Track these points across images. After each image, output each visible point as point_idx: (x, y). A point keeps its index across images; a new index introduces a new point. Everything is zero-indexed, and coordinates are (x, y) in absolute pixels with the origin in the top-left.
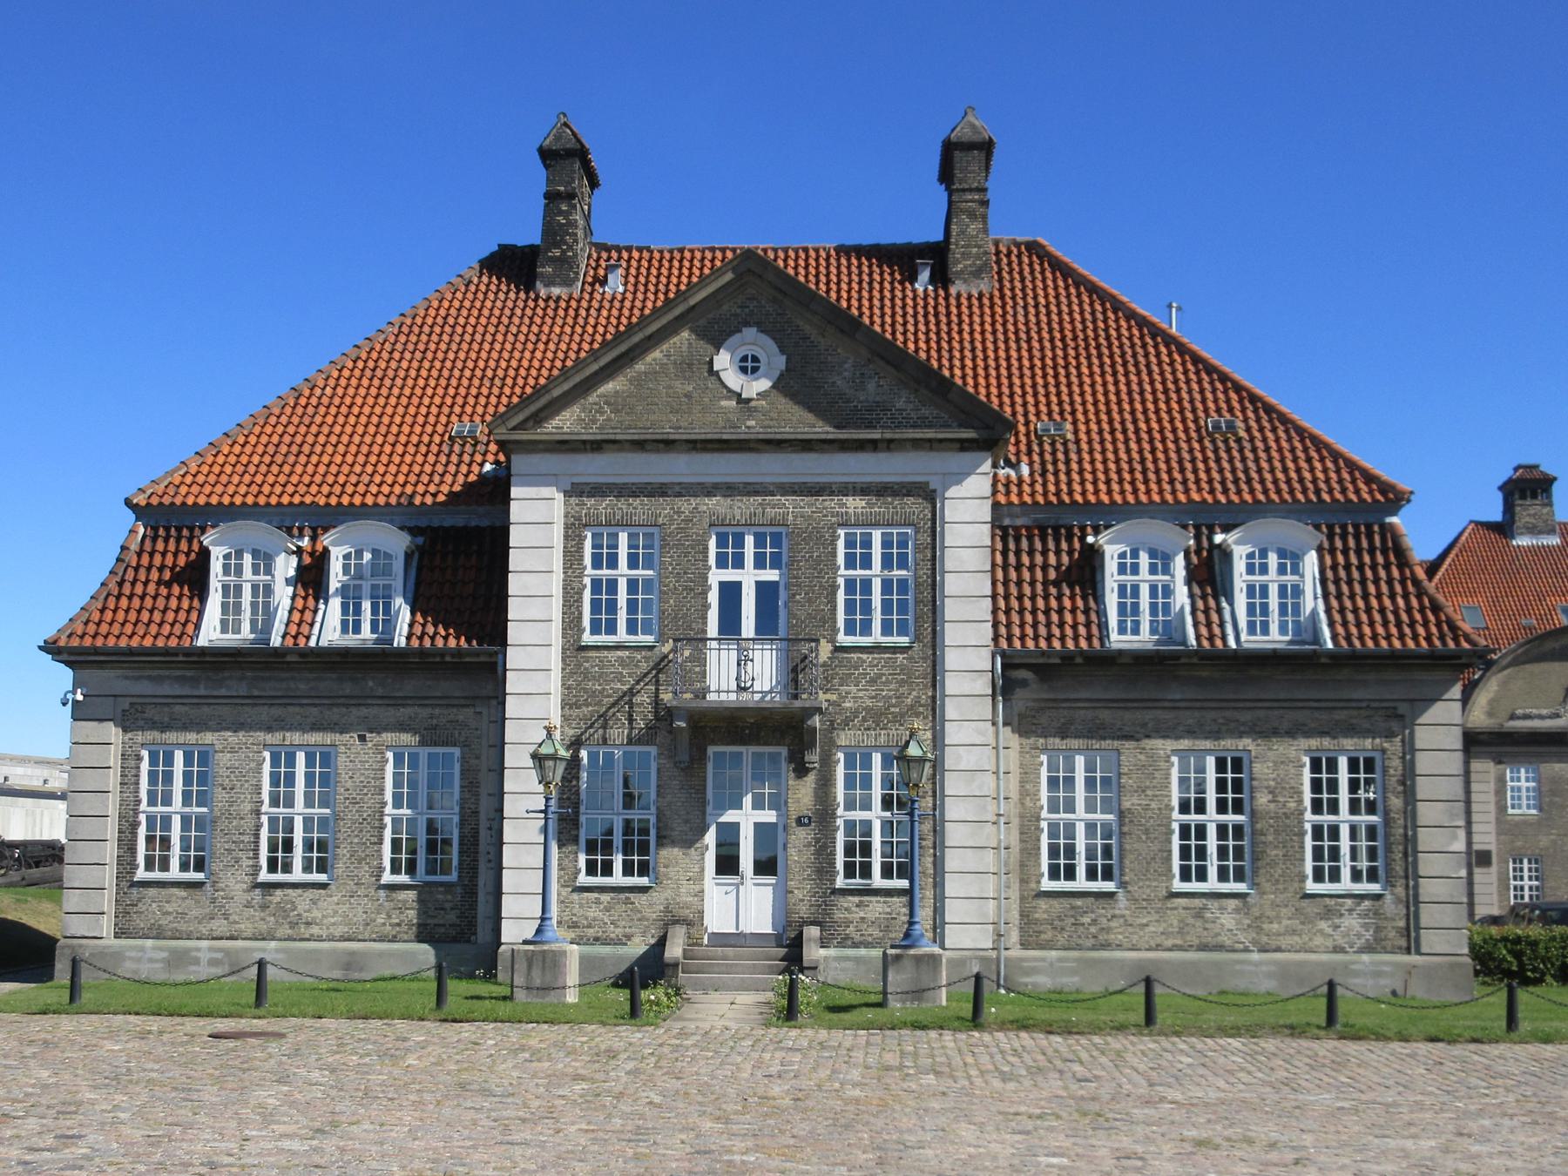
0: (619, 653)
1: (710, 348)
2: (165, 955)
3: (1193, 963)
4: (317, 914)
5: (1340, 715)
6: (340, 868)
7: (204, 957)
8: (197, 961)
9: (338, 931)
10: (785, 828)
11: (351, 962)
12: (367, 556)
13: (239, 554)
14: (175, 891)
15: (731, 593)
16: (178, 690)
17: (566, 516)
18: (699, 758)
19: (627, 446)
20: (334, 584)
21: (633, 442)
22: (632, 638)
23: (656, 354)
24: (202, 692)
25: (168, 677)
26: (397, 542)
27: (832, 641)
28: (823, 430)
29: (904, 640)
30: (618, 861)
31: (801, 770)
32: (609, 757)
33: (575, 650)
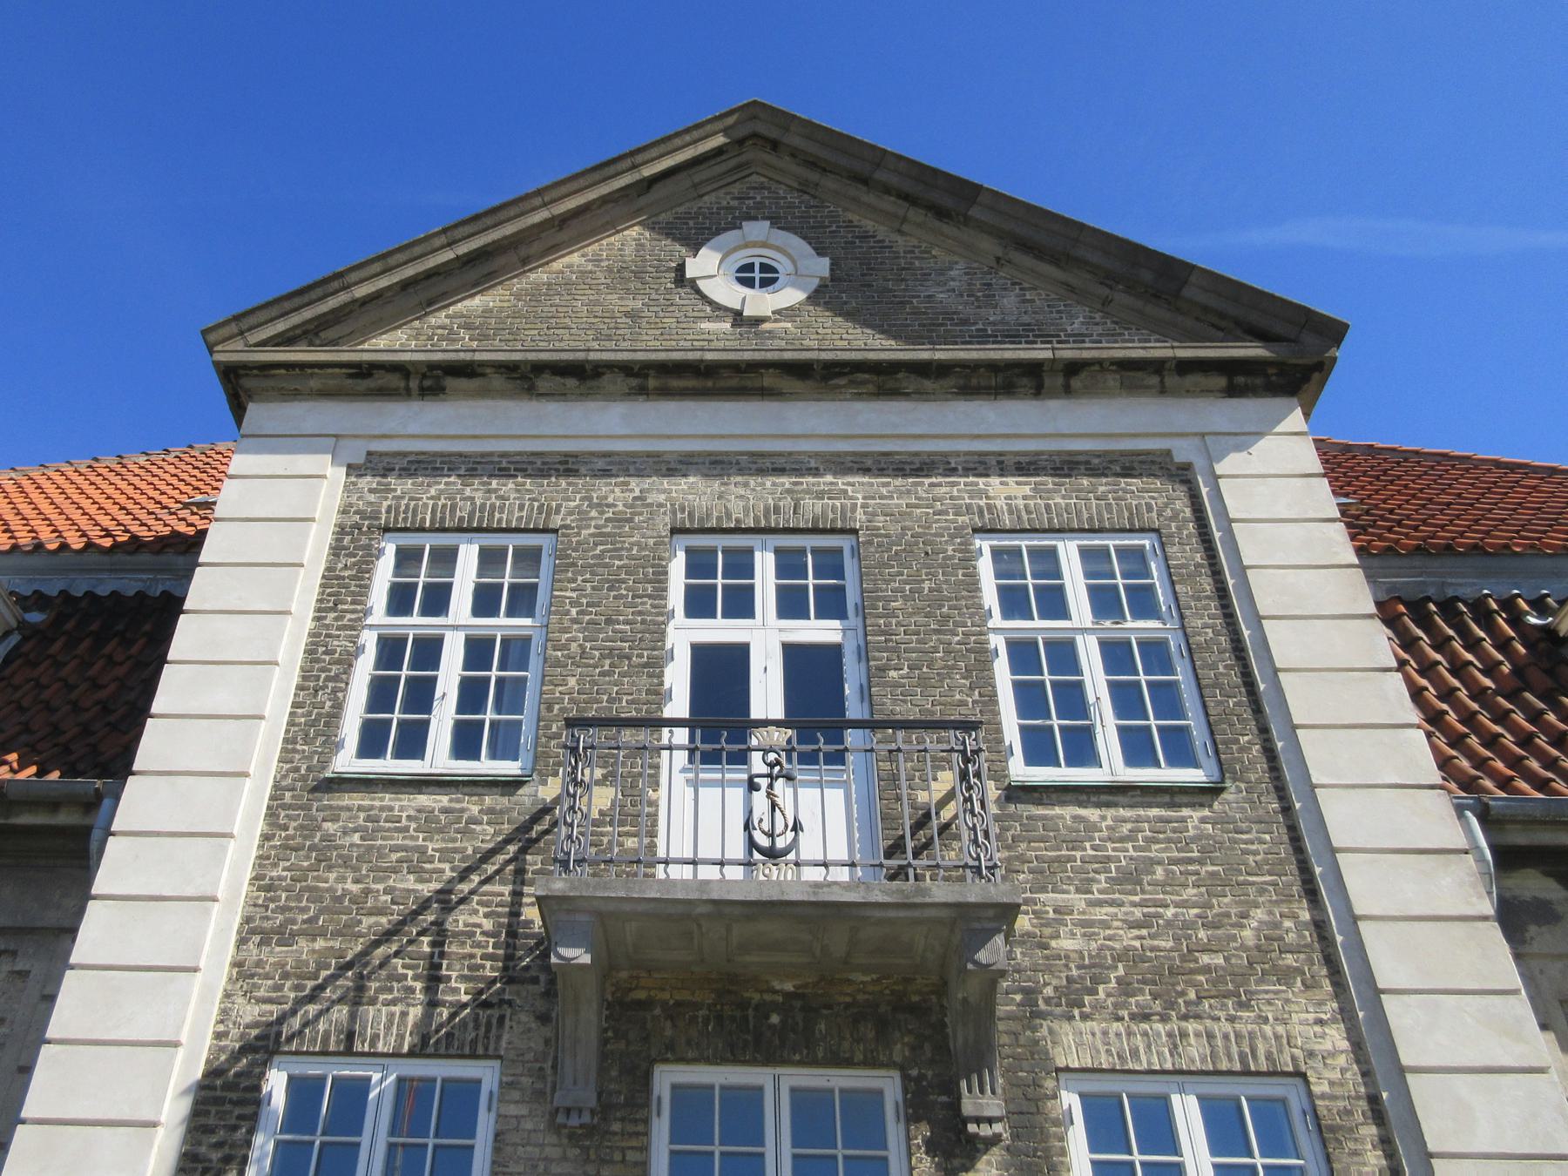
0: (423, 800)
17: (344, 512)
18: (626, 1100)
19: (497, 381)
21: (509, 369)
27: (999, 774)
32: (353, 1094)
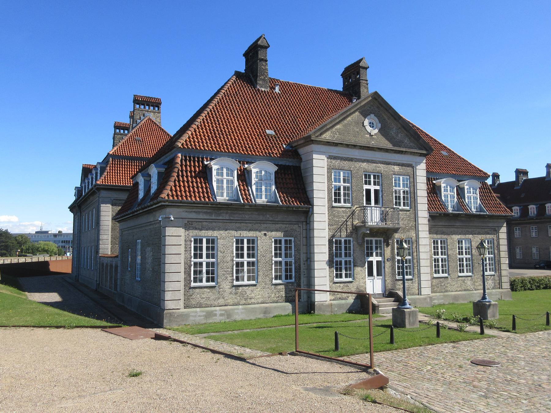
1: (363, 118)
2: (204, 313)
3: (464, 295)
4: (253, 295)
5: (486, 230)
6: (260, 279)
7: (218, 313)
8: (215, 315)
9: (260, 301)
10: (384, 262)
11: (266, 311)
12: (263, 173)
13: (222, 169)
14: (206, 290)
16: (205, 217)
20: (253, 182)
22: (345, 204)
24: (214, 218)
25: (202, 212)
26: (273, 168)
28: (389, 146)
29: (408, 208)
30: (344, 272)
31: (388, 245)
32: (340, 241)
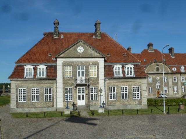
15: (79, 72)
23: (71, 49)
33: (64, 78)
